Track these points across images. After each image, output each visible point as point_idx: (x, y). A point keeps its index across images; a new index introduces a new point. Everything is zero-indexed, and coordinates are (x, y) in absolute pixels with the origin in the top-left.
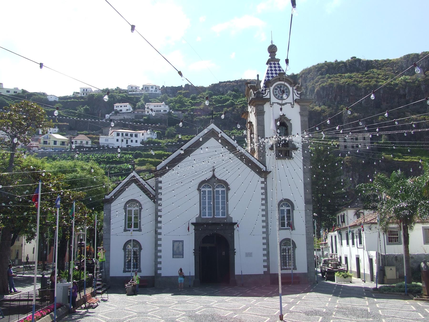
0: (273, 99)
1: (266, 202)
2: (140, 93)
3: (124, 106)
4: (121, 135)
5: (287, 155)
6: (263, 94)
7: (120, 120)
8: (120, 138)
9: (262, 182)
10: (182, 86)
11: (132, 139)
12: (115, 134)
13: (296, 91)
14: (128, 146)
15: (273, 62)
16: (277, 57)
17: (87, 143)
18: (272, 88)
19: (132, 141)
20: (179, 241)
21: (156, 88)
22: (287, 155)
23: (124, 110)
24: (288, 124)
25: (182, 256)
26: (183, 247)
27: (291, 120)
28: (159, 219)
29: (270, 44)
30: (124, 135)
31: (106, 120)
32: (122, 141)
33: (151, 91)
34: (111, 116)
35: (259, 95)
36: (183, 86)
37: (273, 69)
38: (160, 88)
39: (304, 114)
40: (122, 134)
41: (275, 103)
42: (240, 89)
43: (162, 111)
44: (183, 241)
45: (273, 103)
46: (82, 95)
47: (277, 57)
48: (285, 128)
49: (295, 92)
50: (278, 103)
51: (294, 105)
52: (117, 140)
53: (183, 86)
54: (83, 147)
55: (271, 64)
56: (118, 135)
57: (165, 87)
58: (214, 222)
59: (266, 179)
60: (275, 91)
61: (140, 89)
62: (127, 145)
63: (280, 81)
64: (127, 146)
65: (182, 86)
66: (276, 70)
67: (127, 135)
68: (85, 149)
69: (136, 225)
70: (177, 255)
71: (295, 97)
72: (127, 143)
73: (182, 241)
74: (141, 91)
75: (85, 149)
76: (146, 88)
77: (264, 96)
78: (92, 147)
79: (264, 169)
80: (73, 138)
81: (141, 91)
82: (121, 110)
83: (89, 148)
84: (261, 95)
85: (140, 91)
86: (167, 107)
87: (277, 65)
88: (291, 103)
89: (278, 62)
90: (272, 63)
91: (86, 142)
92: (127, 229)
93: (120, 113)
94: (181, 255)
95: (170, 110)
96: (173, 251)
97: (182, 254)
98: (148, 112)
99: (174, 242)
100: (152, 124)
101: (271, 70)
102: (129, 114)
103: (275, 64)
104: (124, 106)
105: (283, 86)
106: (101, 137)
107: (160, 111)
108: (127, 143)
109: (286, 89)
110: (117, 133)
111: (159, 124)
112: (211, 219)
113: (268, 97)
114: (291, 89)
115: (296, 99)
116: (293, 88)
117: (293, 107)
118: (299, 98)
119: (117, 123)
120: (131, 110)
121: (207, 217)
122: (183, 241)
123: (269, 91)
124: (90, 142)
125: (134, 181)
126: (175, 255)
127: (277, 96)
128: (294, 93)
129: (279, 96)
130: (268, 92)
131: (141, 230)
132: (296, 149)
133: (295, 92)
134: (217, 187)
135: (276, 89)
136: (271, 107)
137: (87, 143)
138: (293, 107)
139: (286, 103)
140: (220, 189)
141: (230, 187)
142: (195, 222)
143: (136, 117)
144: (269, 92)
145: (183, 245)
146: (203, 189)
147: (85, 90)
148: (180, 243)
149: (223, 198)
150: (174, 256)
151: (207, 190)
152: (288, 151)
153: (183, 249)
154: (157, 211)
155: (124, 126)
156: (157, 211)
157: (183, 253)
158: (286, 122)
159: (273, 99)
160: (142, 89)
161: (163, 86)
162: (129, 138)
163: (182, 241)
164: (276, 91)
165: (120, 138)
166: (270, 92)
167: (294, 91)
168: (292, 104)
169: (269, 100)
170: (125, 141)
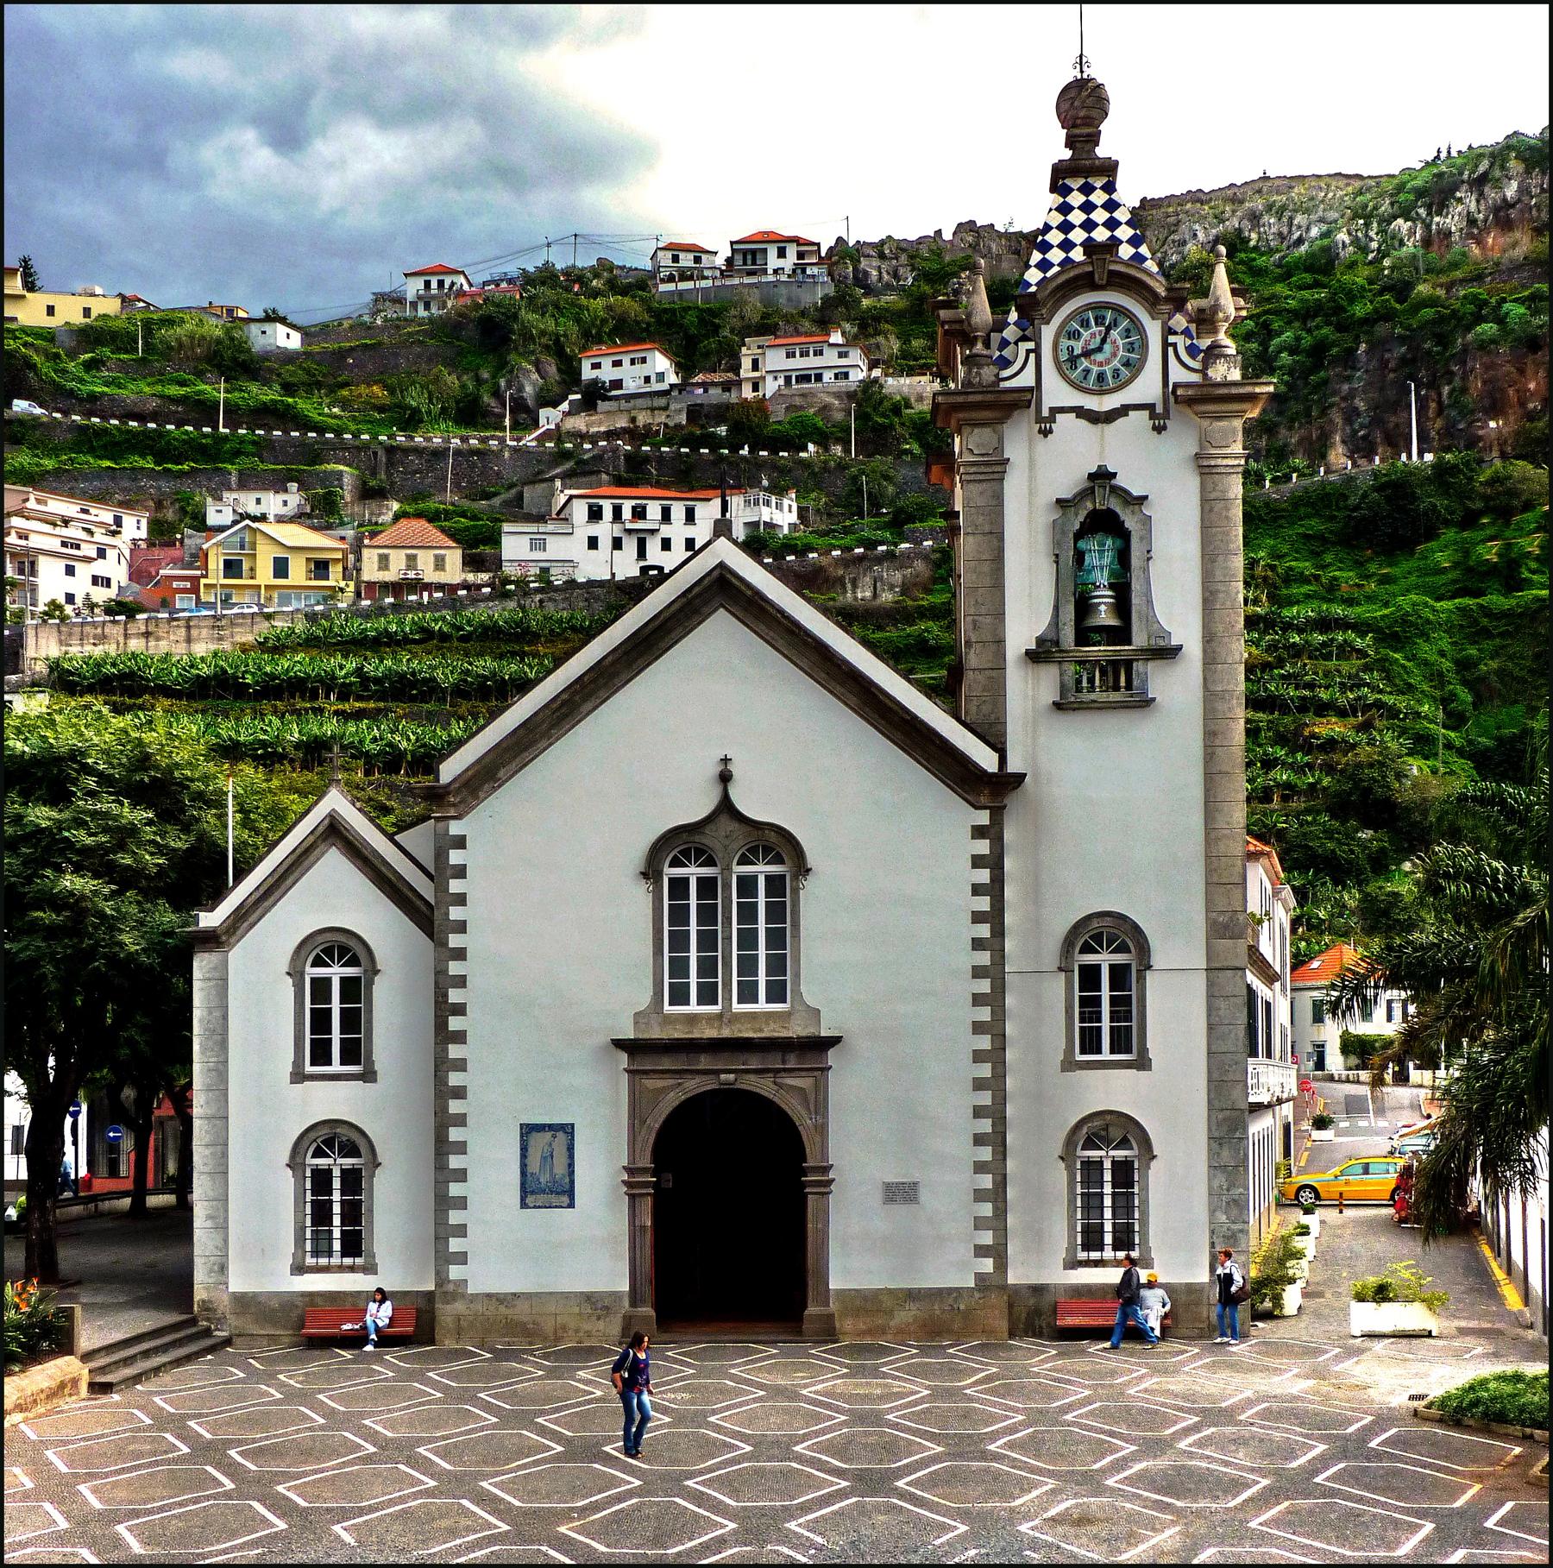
0: (1056, 392)
1: (999, 932)
2: (718, 283)
3: (633, 362)
4: (608, 513)
5: (1123, 683)
6: (1005, 363)
7: (610, 435)
8: (605, 530)
9: (979, 832)
10: (939, 233)
11: (666, 531)
12: (580, 510)
13: (1181, 341)
14: (644, 570)
15: (1081, 181)
16: (1102, 151)
17: (440, 564)
18: (1048, 333)
19: (666, 544)
20: (550, 1126)
21: (801, 255)
22: (1123, 683)
23: (631, 378)
24: (1130, 523)
25: (565, 1199)
26: (571, 1157)
27: (1146, 497)
28: (455, 1023)
29: (1070, 75)
30: (627, 513)
31: (547, 435)
32: (617, 544)
33: (776, 271)
34: (566, 414)
35: (978, 374)
36: (947, 235)
37: (1077, 217)
38: (823, 254)
39: (1220, 462)
40: (617, 512)
41: (1062, 410)
42: (1254, 236)
43: (828, 376)
44: (573, 1125)
45: (1055, 411)
46: (422, 313)
47: (1102, 151)
48: (1119, 542)
49: (1174, 345)
50: (1080, 412)
51: (1166, 414)
52: (593, 543)
53: (947, 235)
54: (417, 585)
55: (1064, 191)
56: (595, 514)
57: (851, 244)
58: (726, 1033)
59: (997, 813)
60: (1065, 343)
61: (720, 261)
62: (643, 563)
63: (1095, 287)
64: (641, 568)
65: (939, 233)
66: (1089, 226)
67: (639, 513)
68: (425, 595)
69: (352, 1053)
70: (543, 1192)
71: (1178, 374)
72: (642, 554)
73: (568, 1130)
74: (722, 272)
75: (425, 595)
76: (748, 253)
77: (1006, 373)
78: (466, 586)
79: (986, 759)
80: (373, 535)
81: (722, 272)
82: (617, 384)
83: (450, 589)
84: (988, 373)
85: (718, 273)
86: (856, 357)
87: (1099, 197)
88: (1149, 407)
89: (1105, 180)
90: (1076, 183)
91: (432, 559)
92: (309, 1069)
93: (617, 398)
94: (563, 1193)
95: (870, 369)
96: (523, 1173)
97: (567, 1187)
98: (755, 388)
99: (528, 1130)
100: (774, 451)
101: (1066, 227)
102: (662, 402)
103: (1087, 190)
104: (633, 362)
105: (1109, 315)
106: (506, 527)
107: (819, 378)
108: (642, 554)
109: (1128, 330)
110: (590, 507)
111: (811, 447)
112: (710, 1018)
113: (1027, 379)
114: (1153, 330)
115: (1176, 386)
116: (1164, 324)
117: (1164, 428)
118: (1195, 378)
119: (596, 452)
120: (673, 378)
121: (693, 1007)
122: (573, 1125)
123: (1031, 345)
124: (454, 557)
125: (333, 831)
126: (533, 1193)
127: (1075, 375)
128: (1171, 349)
129: (1087, 371)
130: (1028, 352)
131: (375, 1073)
132: (1167, 653)
133: (1174, 345)
134: (743, 861)
135: (1075, 335)
136: (1040, 431)
137: (440, 564)
138: (1159, 429)
139: (1124, 410)
140: (761, 870)
141: (812, 859)
142: (630, 1034)
143: (694, 412)
144: (1032, 356)
145: (571, 1149)
146: (670, 872)
147: (434, 285)
148: (554, 1137)
149: (776, 912)
150: (530, 1200)
151: (693, 872)
152: (1128, 664)
153: (571, 1165)
154: (443, 983)
155: (633, 473)
156: (443, 983)
157: (572, 1182)
158: (1118, 510)
159: (1056, 392)
160: (729, 261)
161: (839, 240)
162: (653, 532)
163: (568, 1130)
164: (1072, 343)
165: (605, 530)
166: (1037, 351)
167: (1172, 339)
168: (1159, 409)
169: (1027, 399)
170: (630, 546)
